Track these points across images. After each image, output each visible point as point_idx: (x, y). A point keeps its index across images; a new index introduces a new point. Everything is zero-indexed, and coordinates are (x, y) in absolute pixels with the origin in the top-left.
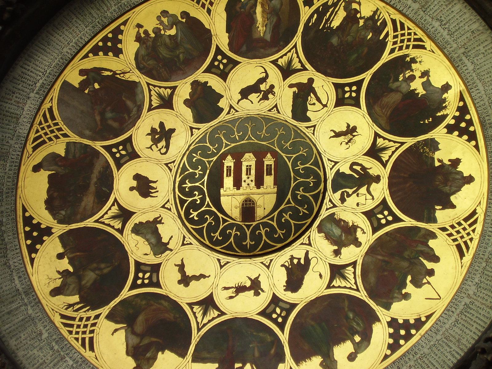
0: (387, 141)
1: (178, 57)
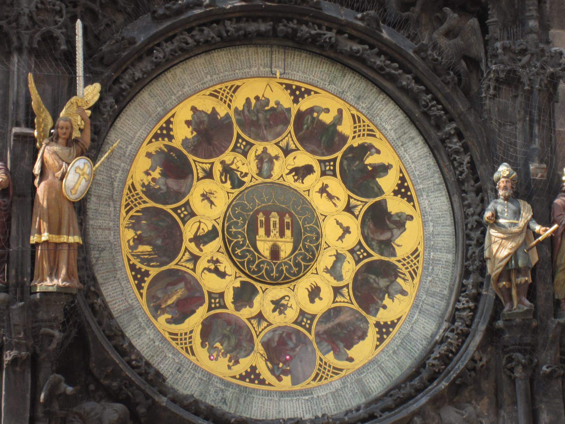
0: (199, 171)
1: (230, 331)
